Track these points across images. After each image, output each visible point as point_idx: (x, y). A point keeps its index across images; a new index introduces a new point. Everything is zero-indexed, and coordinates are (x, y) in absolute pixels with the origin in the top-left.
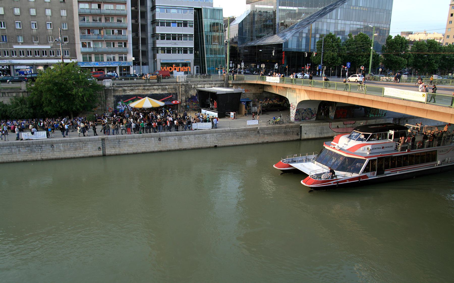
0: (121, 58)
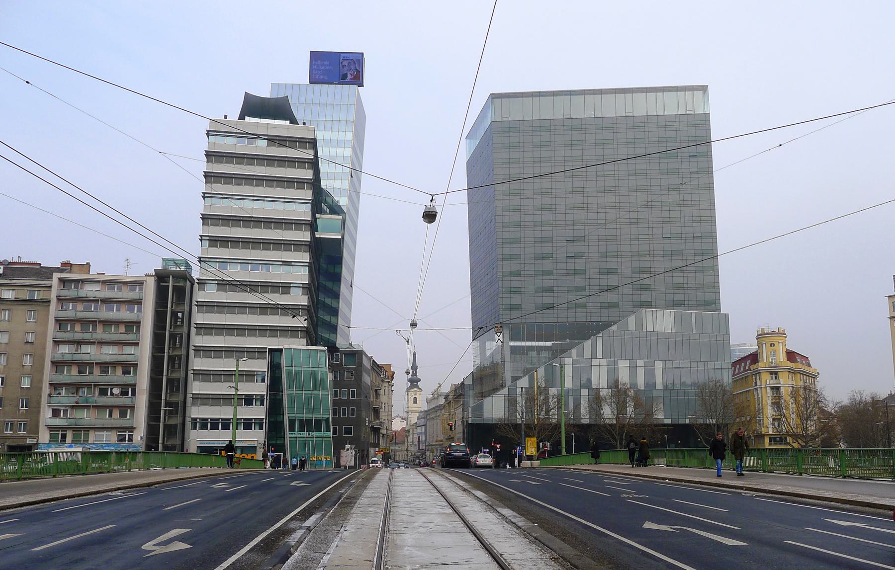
0: (122, 439)
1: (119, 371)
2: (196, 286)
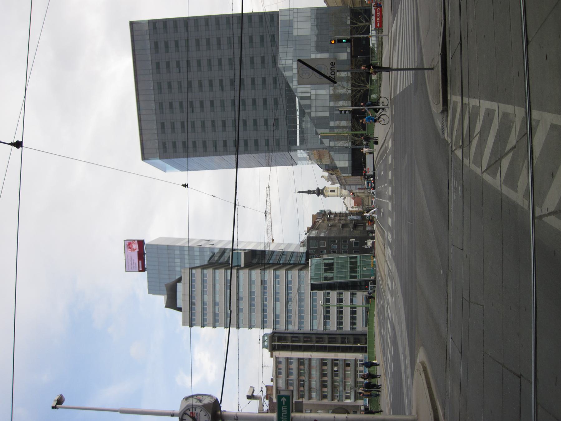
1: (325, 368)
2: (277, 331)
